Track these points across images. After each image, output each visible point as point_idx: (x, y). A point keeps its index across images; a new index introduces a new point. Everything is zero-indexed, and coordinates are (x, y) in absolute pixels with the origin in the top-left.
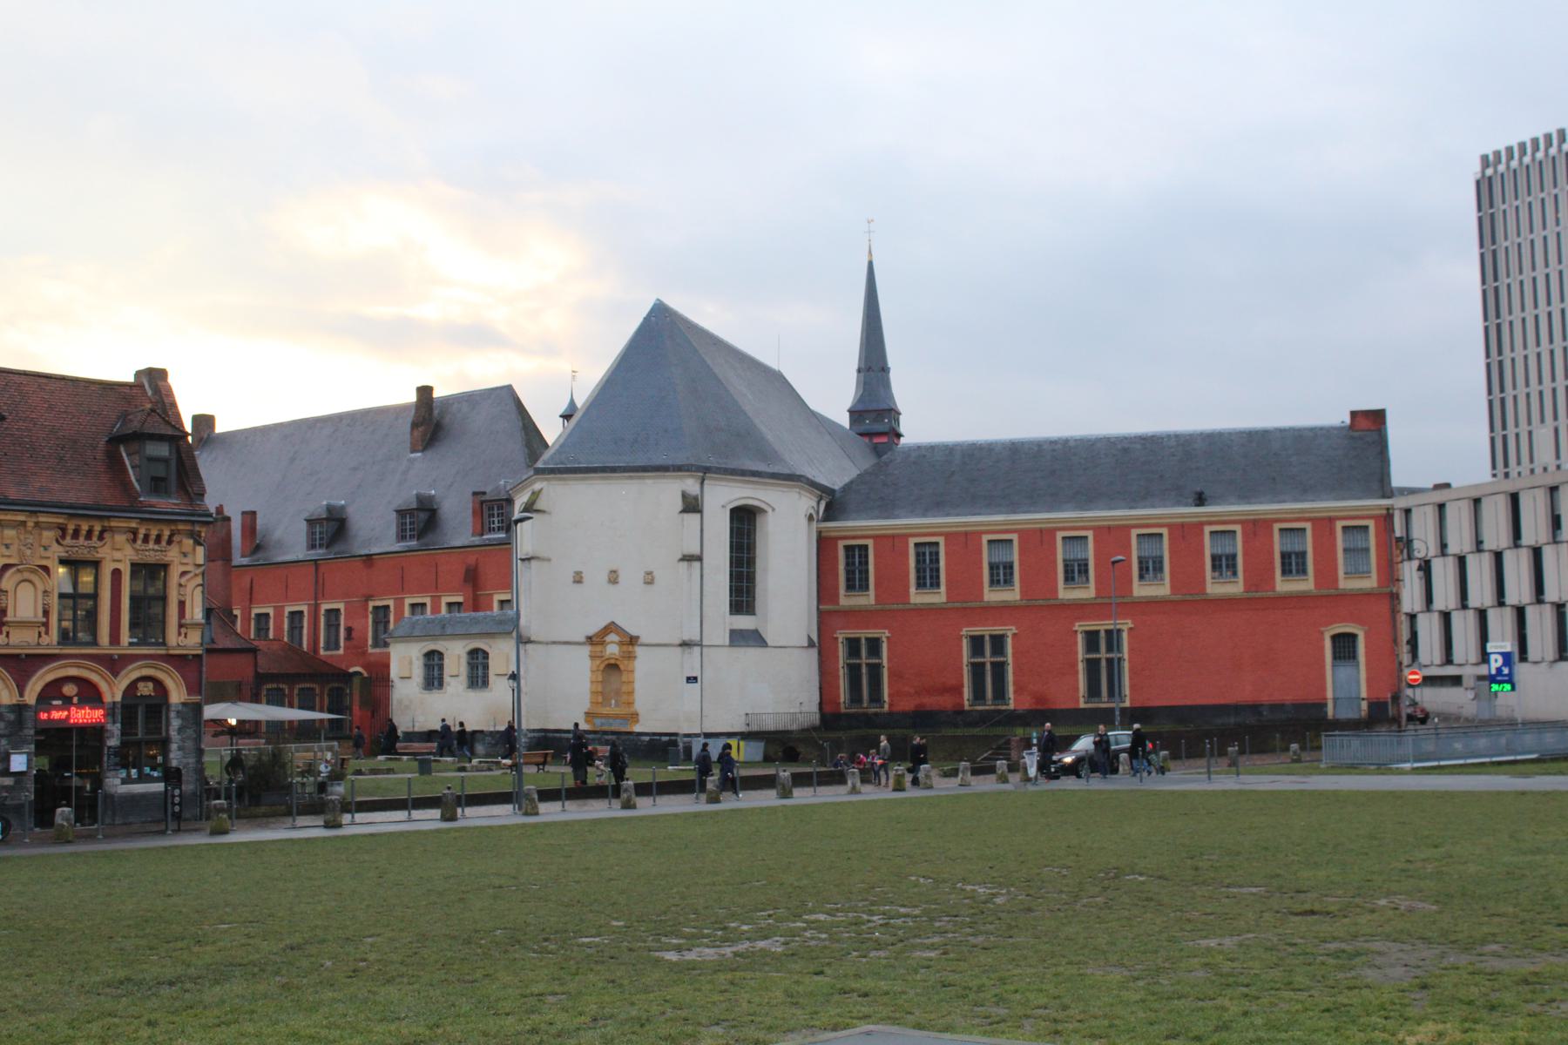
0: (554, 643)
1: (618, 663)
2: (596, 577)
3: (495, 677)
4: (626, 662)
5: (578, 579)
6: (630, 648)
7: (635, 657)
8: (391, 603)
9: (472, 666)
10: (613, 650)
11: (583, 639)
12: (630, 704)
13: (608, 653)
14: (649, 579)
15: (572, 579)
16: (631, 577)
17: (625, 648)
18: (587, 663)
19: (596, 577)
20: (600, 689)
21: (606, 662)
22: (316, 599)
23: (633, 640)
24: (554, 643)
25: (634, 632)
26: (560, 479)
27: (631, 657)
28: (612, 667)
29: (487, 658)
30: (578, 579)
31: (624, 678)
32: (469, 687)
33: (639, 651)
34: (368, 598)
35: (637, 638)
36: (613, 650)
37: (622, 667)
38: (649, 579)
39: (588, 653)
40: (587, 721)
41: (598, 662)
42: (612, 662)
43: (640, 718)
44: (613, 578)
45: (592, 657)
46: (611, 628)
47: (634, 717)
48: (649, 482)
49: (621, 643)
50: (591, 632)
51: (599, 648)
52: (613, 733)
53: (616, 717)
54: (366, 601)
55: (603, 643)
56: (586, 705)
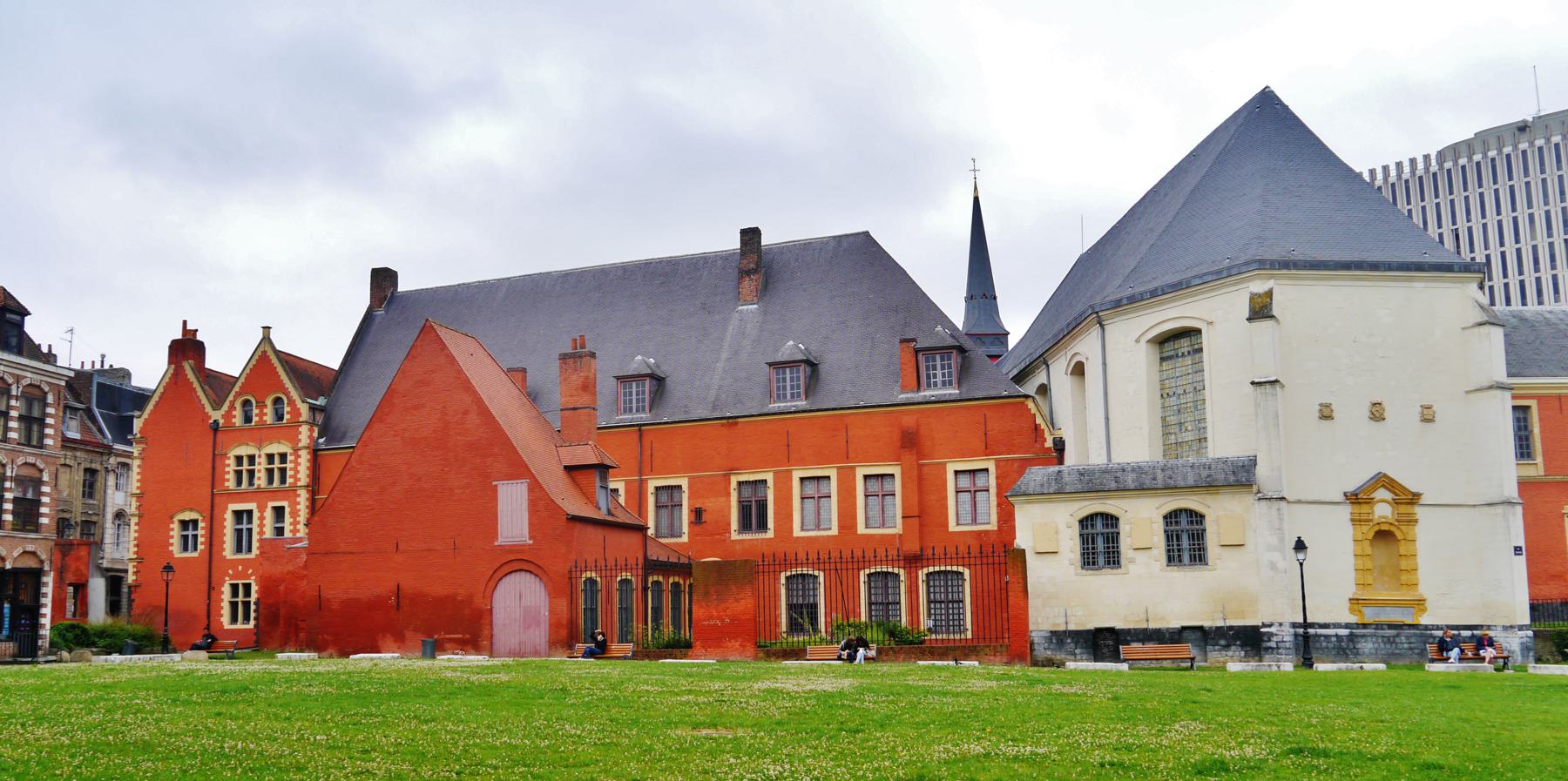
0: (1299, 502)
1: (1392, 529)
2: (1351, 413)
3: (1218, 550)
4: (1402, 527)
5: (1326, 414)
6: (1409, 509)
7: (1416, 521)
8: (769, 477)
10: (1383, 511)
11: (1341, 498)
13: (1376, 517)
14: (1427, 416)
15: (1317, 414)
16: (1402, 414)
17: (1403, 509)
18: (1348, 531)
19: (1351, 413)
21: (1376, 528)
22: (641, 474)
23: (1414, 499)
24: (1299, 502)
26: (1290, 278)
27: (1413, 521)
28: (1384, 536)
30: (1326, 414)
33: (1419, 511)
34: (733, 469)
37: (1398, 534)
38: (1427, 416)
39: (1349, 517)
40: (1352, 611)
41: (1365, 529)
42: (1385, 527)
43: (1427, 604)
44: (1377, 413)
47: (1420, 604)
48: (1419, 285)
49: (1396, 503)
50: (1351, 488)
51: (1365, 509)
52: (1391, 626)
54: (727, 477)
55: (1370, 502)
56: (1351, 590)
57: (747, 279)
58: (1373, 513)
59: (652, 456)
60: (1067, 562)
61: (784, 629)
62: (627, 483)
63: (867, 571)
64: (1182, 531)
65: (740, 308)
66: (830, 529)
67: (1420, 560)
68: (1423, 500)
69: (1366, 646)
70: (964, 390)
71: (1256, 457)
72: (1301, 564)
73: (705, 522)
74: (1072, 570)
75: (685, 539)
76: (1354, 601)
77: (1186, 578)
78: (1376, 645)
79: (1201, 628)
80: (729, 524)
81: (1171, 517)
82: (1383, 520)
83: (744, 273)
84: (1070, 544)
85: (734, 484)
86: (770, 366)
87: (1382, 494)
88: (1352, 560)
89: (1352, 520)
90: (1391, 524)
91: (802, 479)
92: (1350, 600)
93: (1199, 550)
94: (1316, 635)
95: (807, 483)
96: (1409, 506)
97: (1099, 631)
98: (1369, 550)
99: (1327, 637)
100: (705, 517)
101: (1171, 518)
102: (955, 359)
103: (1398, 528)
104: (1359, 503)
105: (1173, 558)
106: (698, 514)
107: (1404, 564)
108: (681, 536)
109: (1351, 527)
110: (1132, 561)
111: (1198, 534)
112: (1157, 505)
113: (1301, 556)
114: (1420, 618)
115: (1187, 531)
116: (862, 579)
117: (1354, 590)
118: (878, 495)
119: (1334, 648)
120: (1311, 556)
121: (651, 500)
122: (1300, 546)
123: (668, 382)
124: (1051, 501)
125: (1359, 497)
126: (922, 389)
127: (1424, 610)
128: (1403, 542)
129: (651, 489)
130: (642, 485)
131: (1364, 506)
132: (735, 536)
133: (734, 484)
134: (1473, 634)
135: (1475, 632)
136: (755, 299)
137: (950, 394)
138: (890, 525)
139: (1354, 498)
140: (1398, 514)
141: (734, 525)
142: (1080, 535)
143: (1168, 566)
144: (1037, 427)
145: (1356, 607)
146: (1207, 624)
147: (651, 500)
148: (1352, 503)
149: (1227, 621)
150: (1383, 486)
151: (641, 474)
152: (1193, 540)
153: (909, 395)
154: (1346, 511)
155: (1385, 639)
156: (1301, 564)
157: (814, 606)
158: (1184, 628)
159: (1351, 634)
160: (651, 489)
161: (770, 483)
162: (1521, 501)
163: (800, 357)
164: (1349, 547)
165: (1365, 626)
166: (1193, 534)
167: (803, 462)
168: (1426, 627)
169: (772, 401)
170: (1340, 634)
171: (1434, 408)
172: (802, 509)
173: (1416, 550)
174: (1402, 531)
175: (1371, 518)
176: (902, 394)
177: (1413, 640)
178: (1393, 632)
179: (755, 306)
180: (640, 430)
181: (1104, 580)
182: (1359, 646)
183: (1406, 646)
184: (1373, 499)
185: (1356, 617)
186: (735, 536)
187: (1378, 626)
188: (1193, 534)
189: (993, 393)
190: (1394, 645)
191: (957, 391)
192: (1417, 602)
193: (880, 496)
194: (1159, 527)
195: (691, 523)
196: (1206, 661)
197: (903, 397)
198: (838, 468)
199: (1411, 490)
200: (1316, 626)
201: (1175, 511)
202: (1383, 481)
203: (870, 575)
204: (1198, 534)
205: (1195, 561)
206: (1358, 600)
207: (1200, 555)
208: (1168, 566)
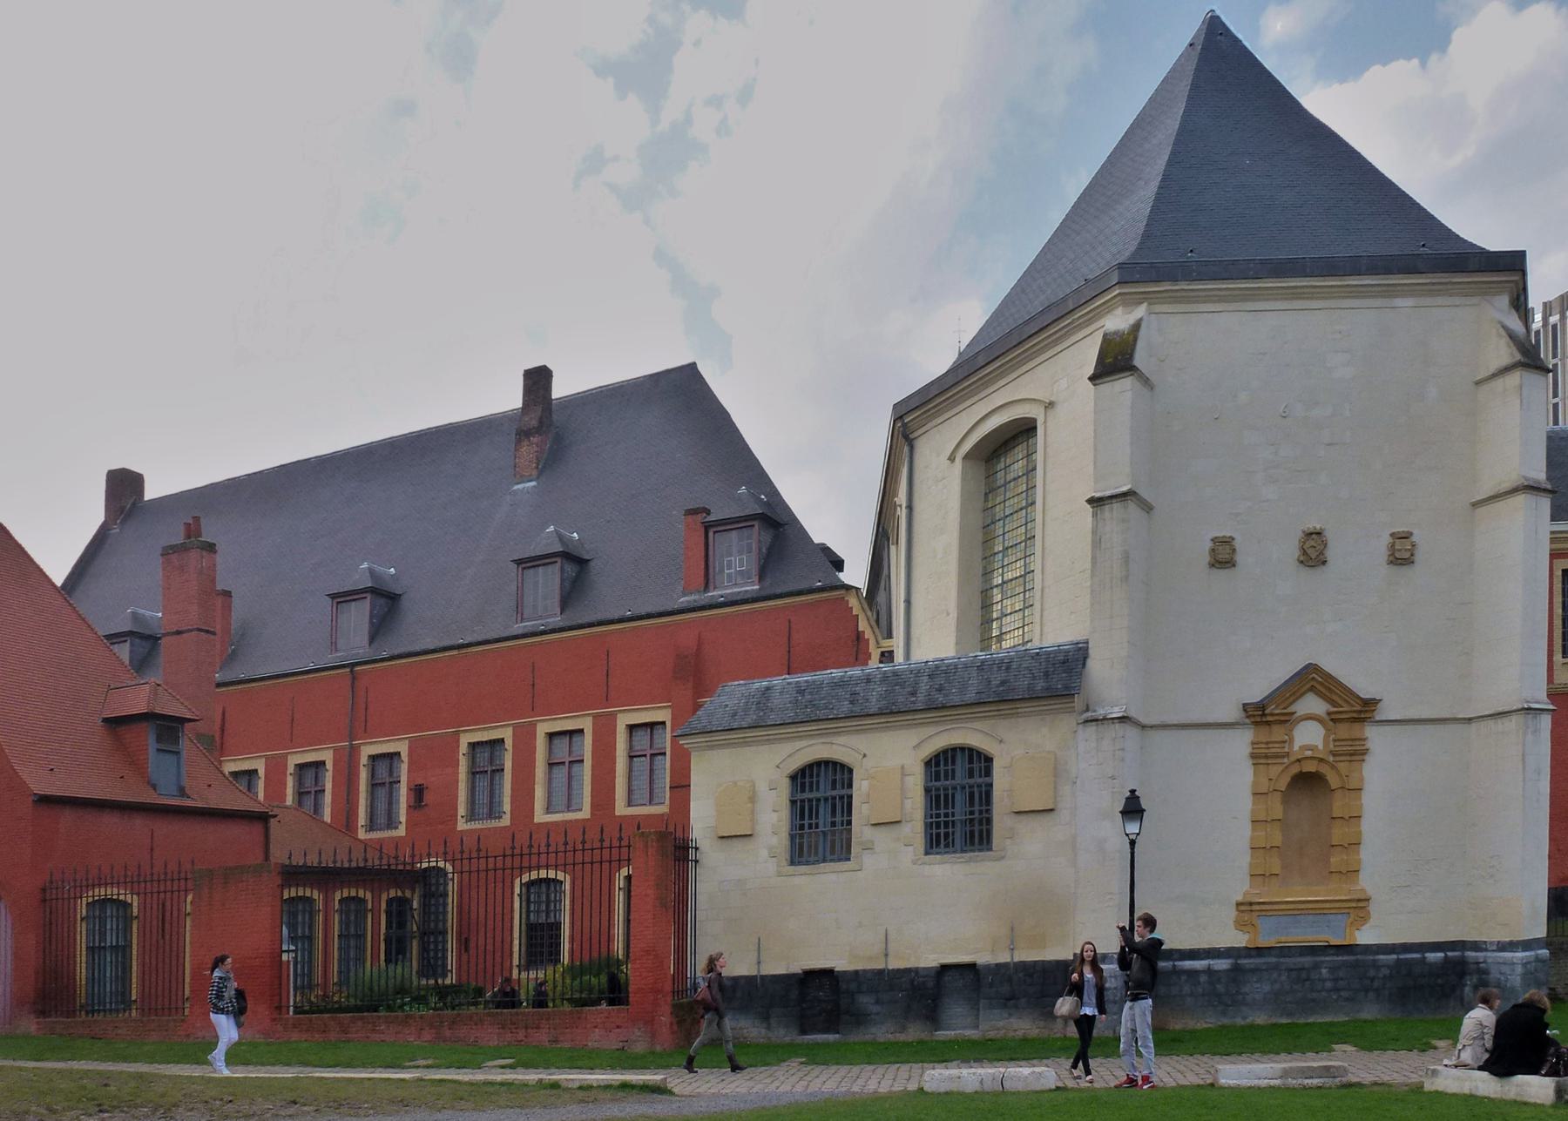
1: (1324, 770)
4: (1342, 766)
9: (936, 799)
12: (1352, 873)
13: (1296, 748)
14: (1401, 553)
17: (1344, 731)
20: (1277, 839)
21: (1295, 770)
23: (1364, 710)
25: (1363, 687)
27: (1358, 753)
28: (1308, 782)
29: (988, 772)
31: (1338, 806)
32: (792, 863)
33: (1374, 736)
35: (1370, 704)
36: (1309, 737)
37: (1334, 781)
38: (1401, 553)
39: (1247, 750)
40: (1240, 925)
41: (1275, 770)
42: (1310, 767)
43: (1373, 908)
45: (1259, 757)
46: (1311, 679)
49: (1334, 719)
50: (1256, 694)
51: (1278, 733)
53: (1318, 910)
55: (1288, 720)
56: (1240, 888)
57: (526, 443)
58: (1291, 740)
59: (366, 709)
60: (764, 853)
61: (516, 962)
62: (336, 750)
63: (525, 878)
64: (954, 788)
65: (516, 487)
66: (581, 810)
67: (1367, 826)
68: (1385, 712)
69: (1257, 989)
70: (768, 582)
71: (1087, 643)
72: (1132, 843)
73: (426, 805)
74: (772, 867)
75: (401, 831)
76: (1245, 907)
77: (950, 871)
78: (1277, 986)
79: (971, 967)
80: (456, 809)
81: (939, 764)
82: (1309, 753)
83: (523, 434)
84: (773, 818)
85: (463, 748)
86: (518, 564)
87: (1312, 704)
88: (1246, 830)
89: (1253, 756)
90: (1321, 760)
91: (551, 736)
92: (1239, 904)
93: (946, 824)
94: (1177, 972)
95: (556, 741)
96: (1357, 726)
97: (810, 975)
98: (1277, 810)
99: (1193, 973)
100: (428, 798)
101: (937, 764)
102: (756, 537)
103: (1333, 767)
104: (1268, 723)
105: (939, 838)
106: (418, 792)
107: (1338, 834)
108: (396, 828)
109: (1252, 767)
110: (868, 847)
111: (946, 796)
112: (915, 741)
113: (1133, 828)
114: (1357, 933)
115: (963, 788)
116: (517, 890)
117: (1246, 887)
118: (645, 756)
119: (1203, 995)
120: (1150, 829)
121: (363, 775)
122: (1133, 809)
123: (405, 603)
124: (746, 743)
125: (1267, 712)
126: (711, 587)
127: (1364, 919)
128: (1338, 794)
129: (364, 760)
130: (354, 752)
131: (1275, 728)
132: (462, 825)
133: (463, 748)
134: (1398, 959)
135: (1449, 954)
136: (535, 473)
137: (746, 591)
138: (639, 802)
139: (1260, 715)
140: (1335, 740)
141: (462, 810)
142: (793, 802)
143: (927, 853)
144: (859, 636)
145: (1246, 917)
146: (983, 958)
147: (363, 775)
148: (1256, 723)
149: (1016, 953)
150: (1312, 689)
151: (352, 738)
152: (938, 807)
153: (693, 597)
154: (1241, 742)
155: (1294, 974)
156: (1132, 843)
157: (556, 926)
158: (945, 968)
159: (1236, 969)
160: (364, 760)
161: (509, 744)
162: (1551, 707)
163: (558, 548)
164: (1244, 804)
165: (1259, 951)
166: (938, 797)
167: (551, 710)
168: (1368, 949)
169: (519, 621)
170: (1216, 968)
171: (1414, 539)
172: (550, 781)
173: (1361, 806)
174: (1338, 771)
175: (1286, 750)
176: (684, 595)
177: (1341, 974)
178: (1307, 960)
179: (533, 483)
180: (352, 671)
181: (824, 880)
182: (1246, 989)
183: (1329, 985)
184: (1293, 713)
185: (1246, 937)
186: (462, 825)
187: (1284, 951)
188: (938, 797)
189: (804, 585)
190: (1308, 983)
191: (757, 587)
192: (1354, 905)
193: (648, 756)
194: (916, 783)
195: (409, 807)
196: (977, 1027)
197: (685, 600)
198: (595, 717)
199: (1362, 696)
200: (1175, 956)
201: (945, 752)
202: (1311, 679)
203: (531, 883)
204: (946, 796)
205: (938, 844)
206: (1251, 904)
207: (947, 835)
208: (927, 853)
